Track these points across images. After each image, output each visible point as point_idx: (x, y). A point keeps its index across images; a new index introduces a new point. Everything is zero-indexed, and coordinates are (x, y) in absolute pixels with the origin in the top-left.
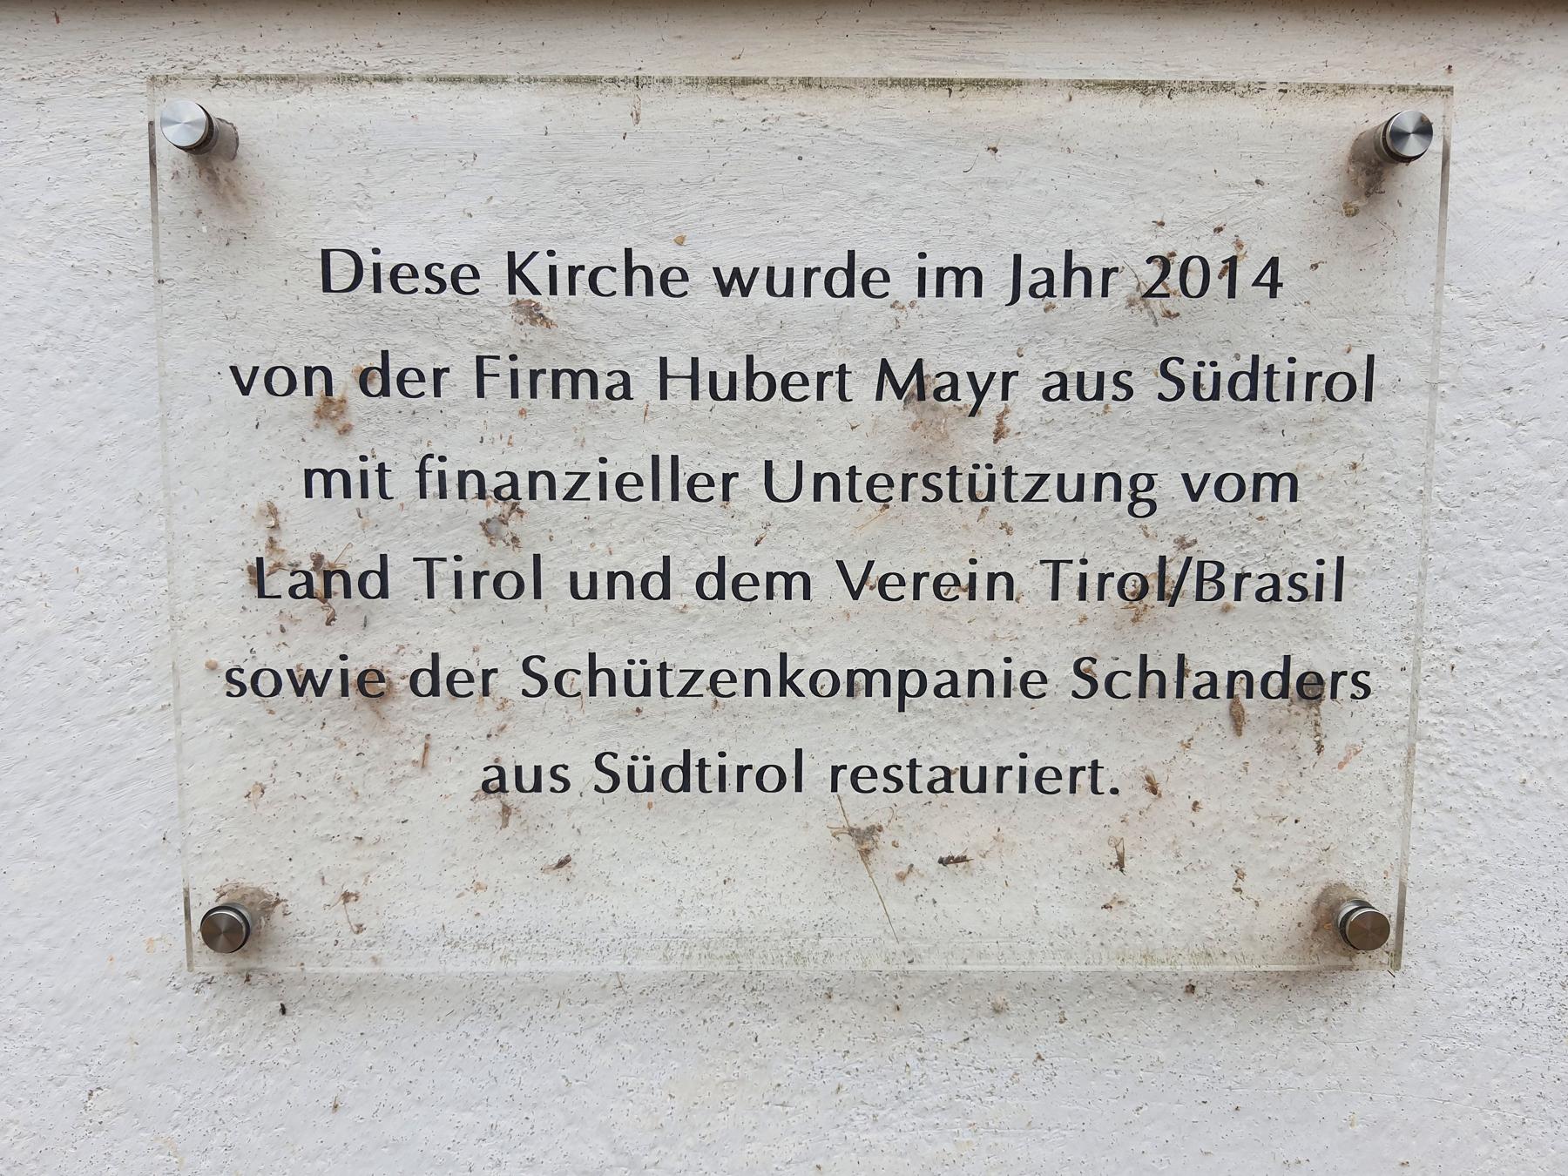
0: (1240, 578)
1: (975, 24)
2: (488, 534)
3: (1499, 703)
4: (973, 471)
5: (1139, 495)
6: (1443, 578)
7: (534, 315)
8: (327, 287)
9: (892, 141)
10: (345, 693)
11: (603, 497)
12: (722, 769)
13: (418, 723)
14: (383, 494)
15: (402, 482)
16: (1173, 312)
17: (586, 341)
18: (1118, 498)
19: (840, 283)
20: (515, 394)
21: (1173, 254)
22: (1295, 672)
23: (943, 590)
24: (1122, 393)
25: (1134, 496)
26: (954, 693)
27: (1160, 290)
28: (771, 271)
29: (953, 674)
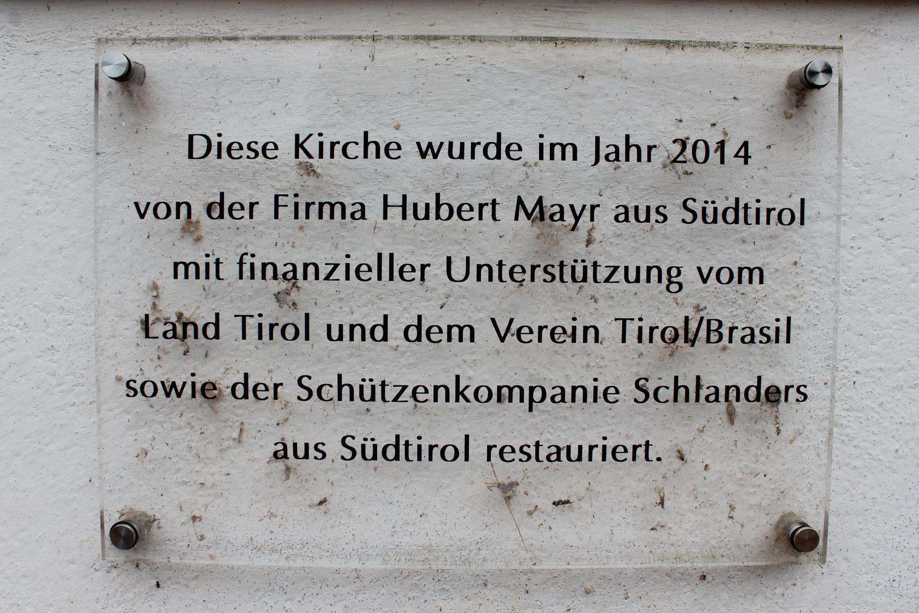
0: (732, 329)
1: (571, 7)
2: (278, 301)
3: (881, 404)
4: (574, 264)
5: (673, 279)
6: (848, 330)
7: (310, 170)
8: (191, 156)
9: (523, 71)
10: (194, 396)
11: (348, 278)
12: (419, 447)
13: (236, 415)
14: (218, 277)
15: (229, 270)
16: (689, 171)
17: (340, 186)
18: (660, 281)
19: (492, 151)
20: (296, 217)
21: (688, 138)
22: (764, 385)
23: (556, 336)
24: (661, 218)
25: (669, 280)
26: (563, 400)
27: (681, 158)
28: (451, 144)
29: (562, 389)
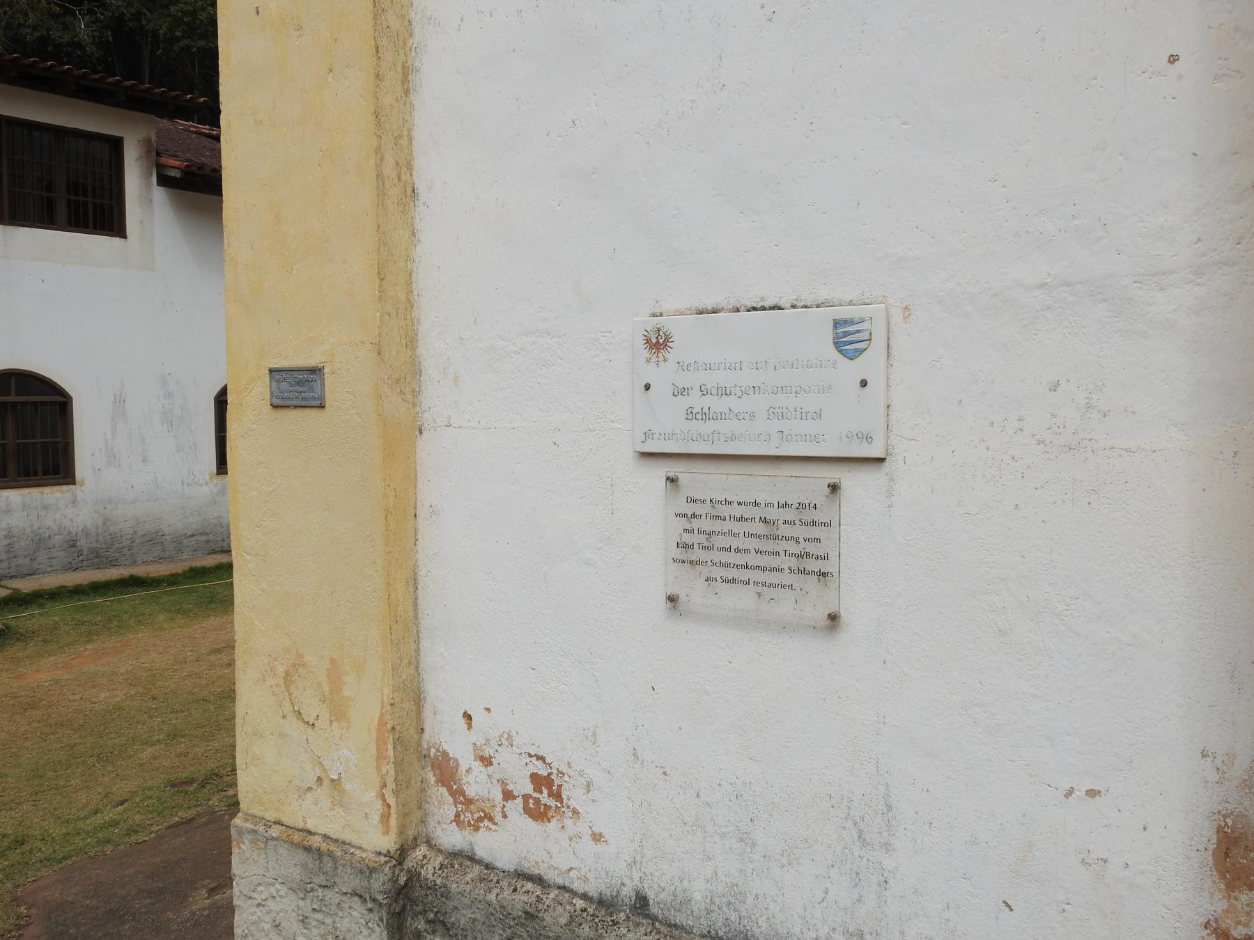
0: (813, 555)
7: (713, 507)
15: (696, 531)
